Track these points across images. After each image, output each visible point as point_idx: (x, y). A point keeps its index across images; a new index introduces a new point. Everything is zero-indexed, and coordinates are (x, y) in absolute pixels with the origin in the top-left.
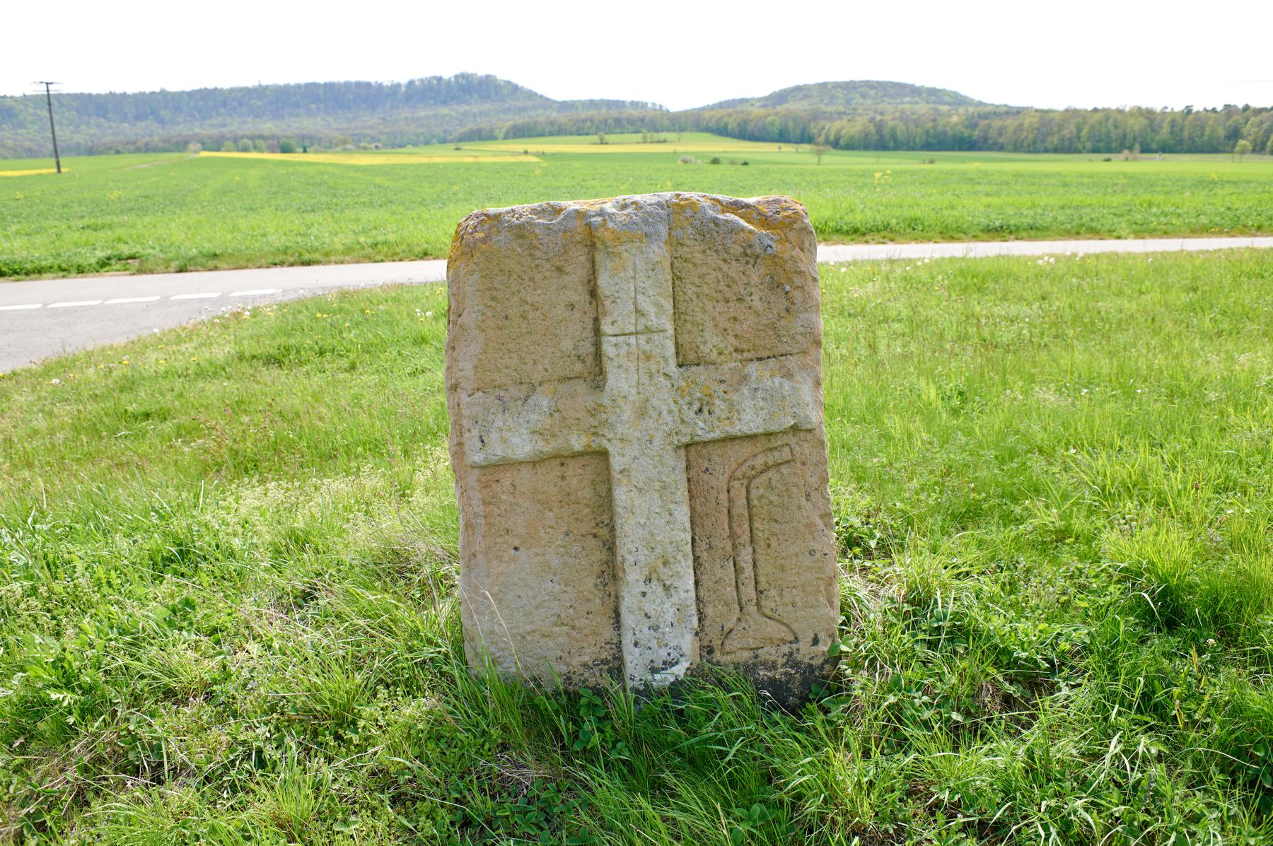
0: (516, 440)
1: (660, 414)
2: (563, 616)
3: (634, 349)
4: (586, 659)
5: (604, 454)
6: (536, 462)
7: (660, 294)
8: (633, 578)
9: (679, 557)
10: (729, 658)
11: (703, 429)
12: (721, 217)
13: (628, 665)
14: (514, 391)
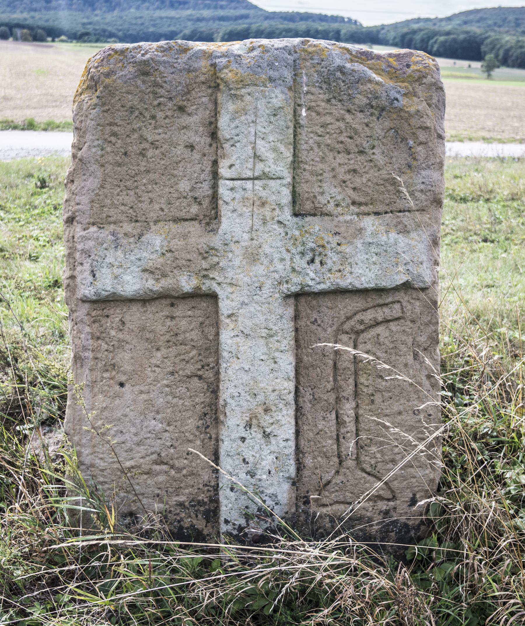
0: (127, 278)
1: (271, 261)
2: (163, 455)
3: (249, 194)
4: (182, 498)
5: (213, 297)
6: (145, 300)
7: (281, 141)
8: (233, 423)
9: (281, 406)
10: (324, 510)
11: (313, 278)
12: (348, 65)
13: (223, 509)
14: (128, 227)
